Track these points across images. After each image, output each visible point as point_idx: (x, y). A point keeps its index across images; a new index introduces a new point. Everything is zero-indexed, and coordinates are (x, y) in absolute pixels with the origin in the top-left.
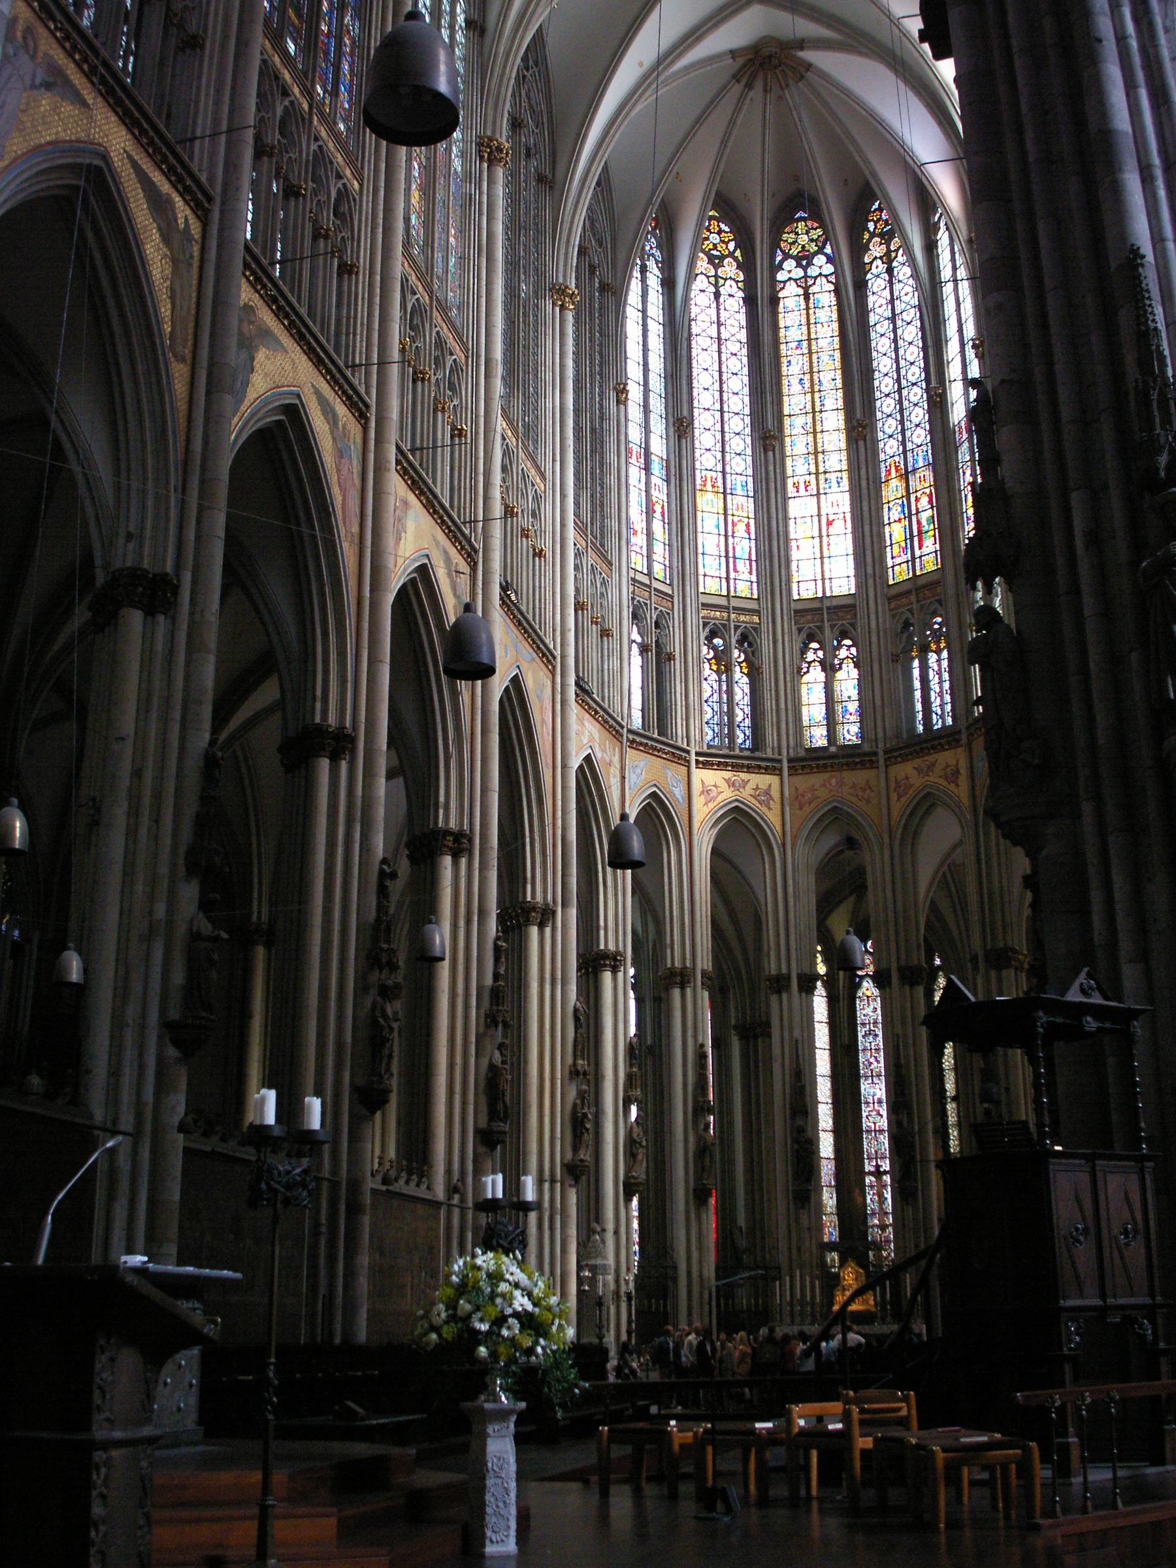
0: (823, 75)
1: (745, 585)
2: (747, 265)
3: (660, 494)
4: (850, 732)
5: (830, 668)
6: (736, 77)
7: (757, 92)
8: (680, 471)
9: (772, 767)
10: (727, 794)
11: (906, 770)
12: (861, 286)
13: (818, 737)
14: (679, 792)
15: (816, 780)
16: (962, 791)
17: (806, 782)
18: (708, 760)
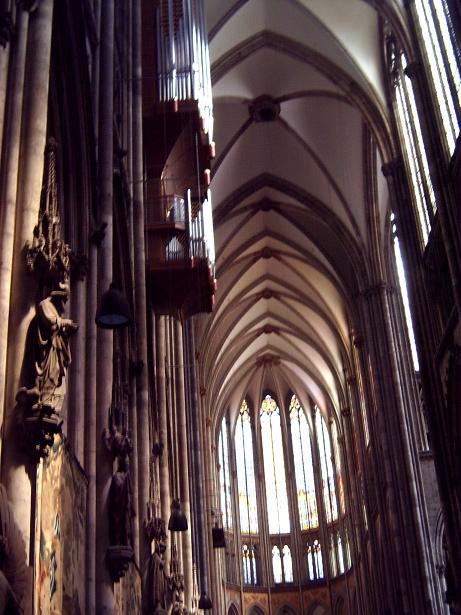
0: (284, 365)
1: (255, 529)
2: (252, 414)
3: (229, 499)
4: (289, 578)
5: (282, 555)
6: (256, 363)
7: (262, 368)
8: (234, 490)
9: (265, 591)
10: (252, 601)
11: (309, 593)
12: (289, 425)
13: (278, 579)
14: (238, 602)
15: (280, 595)
16: (328, 601)
17: (275, 596)
18: (250, 588)
